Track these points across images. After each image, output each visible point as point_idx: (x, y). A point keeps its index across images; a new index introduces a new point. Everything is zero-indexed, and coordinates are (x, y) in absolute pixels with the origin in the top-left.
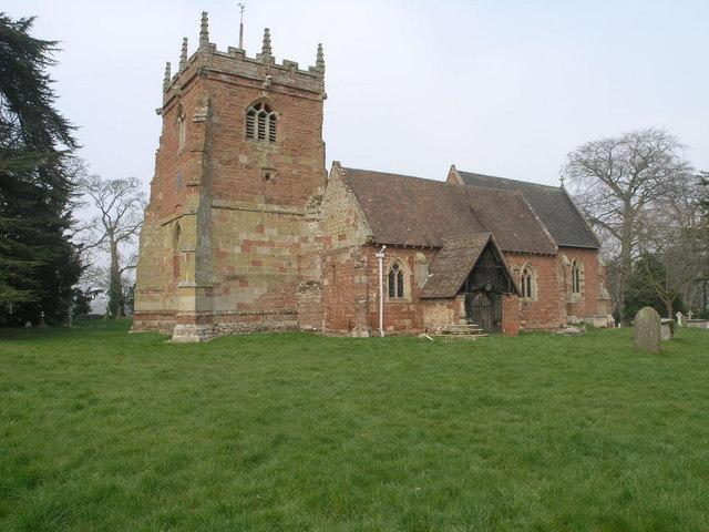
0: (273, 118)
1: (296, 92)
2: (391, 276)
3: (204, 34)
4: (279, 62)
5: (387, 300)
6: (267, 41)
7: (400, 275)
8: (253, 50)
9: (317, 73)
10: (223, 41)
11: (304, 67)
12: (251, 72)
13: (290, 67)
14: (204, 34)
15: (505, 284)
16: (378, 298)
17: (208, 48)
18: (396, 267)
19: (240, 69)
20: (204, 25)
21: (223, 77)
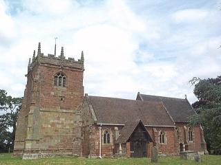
0: (64, 78)
1: (73, 69)
2: (105, 135)
3: (39, 50)
4: (67, 58)
5: (103, 144)
6: (62, 51)
7: (109, 135)
8: (58, 54)
9: (81, 62)
10: (46, 51)
11: (76, 60)
12: (56, 63)
13: (71, 60)
14: (39, 50)
15: (148, 139)
16: (99, 144)
17: (41, 55)
18: (107, 132)
19: (52, 61)
20: (39, 47)
21: (46, 65)
